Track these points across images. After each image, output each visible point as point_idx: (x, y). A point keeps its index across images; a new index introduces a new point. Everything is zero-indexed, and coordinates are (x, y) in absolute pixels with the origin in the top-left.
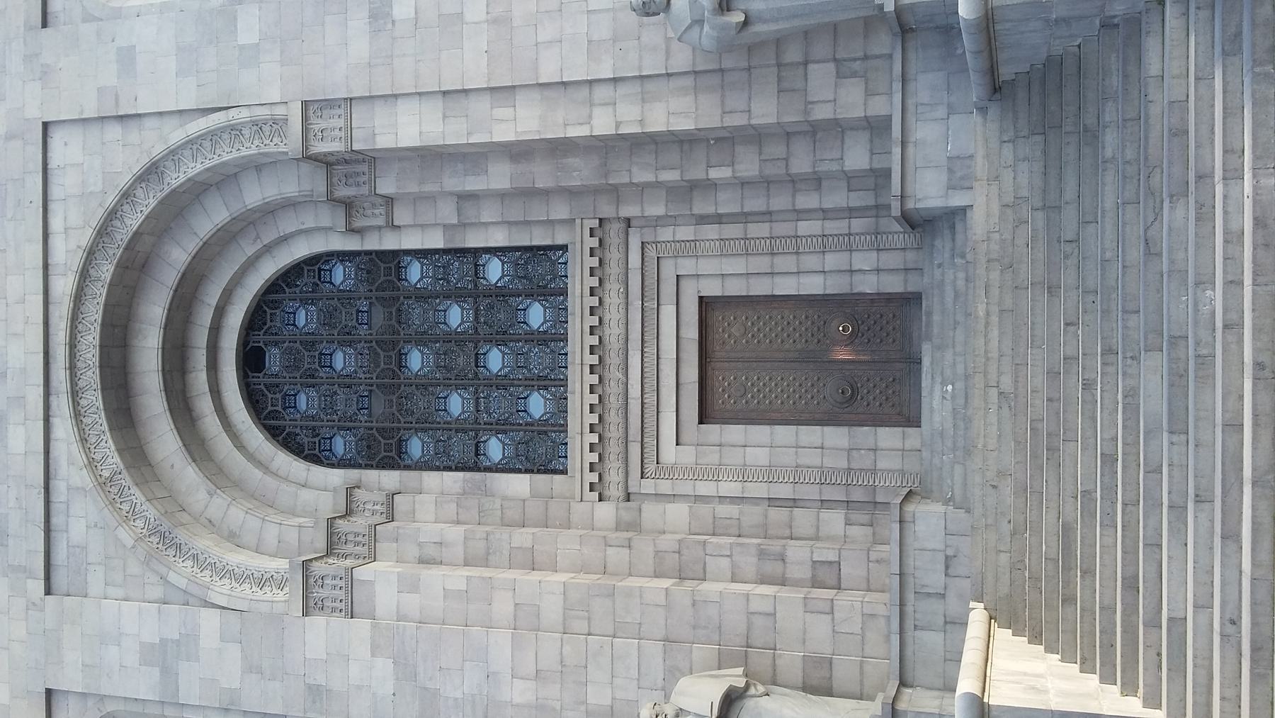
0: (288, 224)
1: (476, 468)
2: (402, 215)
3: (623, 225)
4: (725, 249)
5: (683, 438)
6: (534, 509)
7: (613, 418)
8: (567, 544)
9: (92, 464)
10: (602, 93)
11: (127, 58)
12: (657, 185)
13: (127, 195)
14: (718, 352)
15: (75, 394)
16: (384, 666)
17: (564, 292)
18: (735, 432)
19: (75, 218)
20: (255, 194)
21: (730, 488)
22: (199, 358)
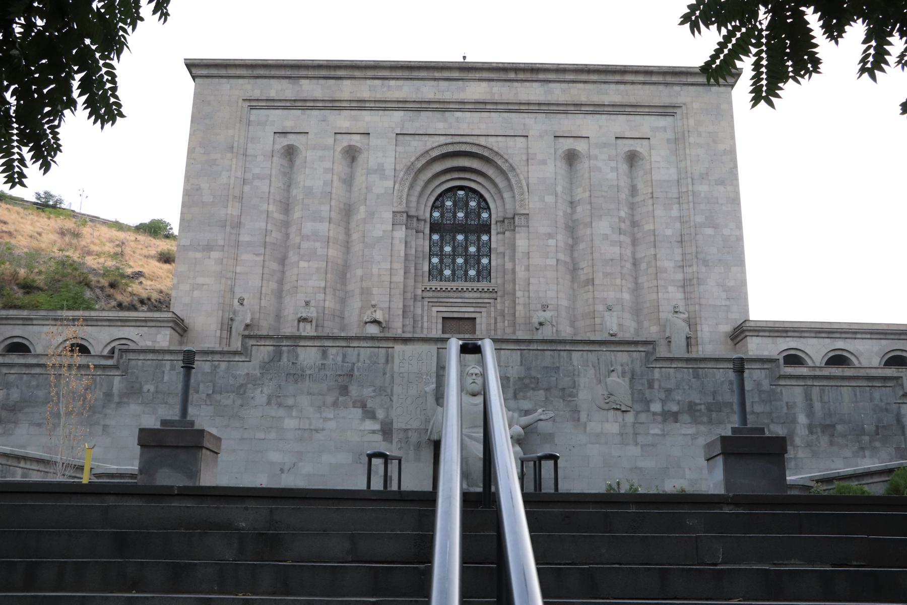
0: (499, 203)
1: (430, 255)
2: (500, 236)
3: (495, 297)
4: (488, 324)
5: (439, 313)
6: (420, 273)
7: (444, 294)
8: (411, 282)
9: (433, 148)
10: (526, 294)
11: (544, 162)
12: (505, 307)
13: (507, 161)
14: (461, 322)
15: (452, 143)
16: (380, 234)
17: (478, 281)
18: (440, 326)
19: (501, 145)
20: (507, 195)
21: (425, 325)
22: (462, 175)
